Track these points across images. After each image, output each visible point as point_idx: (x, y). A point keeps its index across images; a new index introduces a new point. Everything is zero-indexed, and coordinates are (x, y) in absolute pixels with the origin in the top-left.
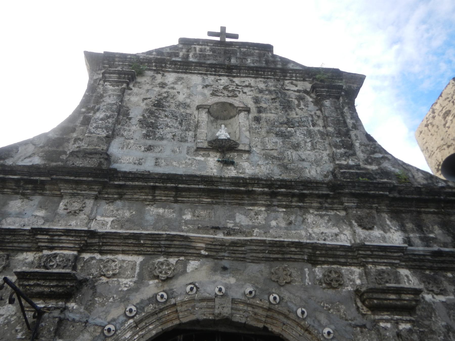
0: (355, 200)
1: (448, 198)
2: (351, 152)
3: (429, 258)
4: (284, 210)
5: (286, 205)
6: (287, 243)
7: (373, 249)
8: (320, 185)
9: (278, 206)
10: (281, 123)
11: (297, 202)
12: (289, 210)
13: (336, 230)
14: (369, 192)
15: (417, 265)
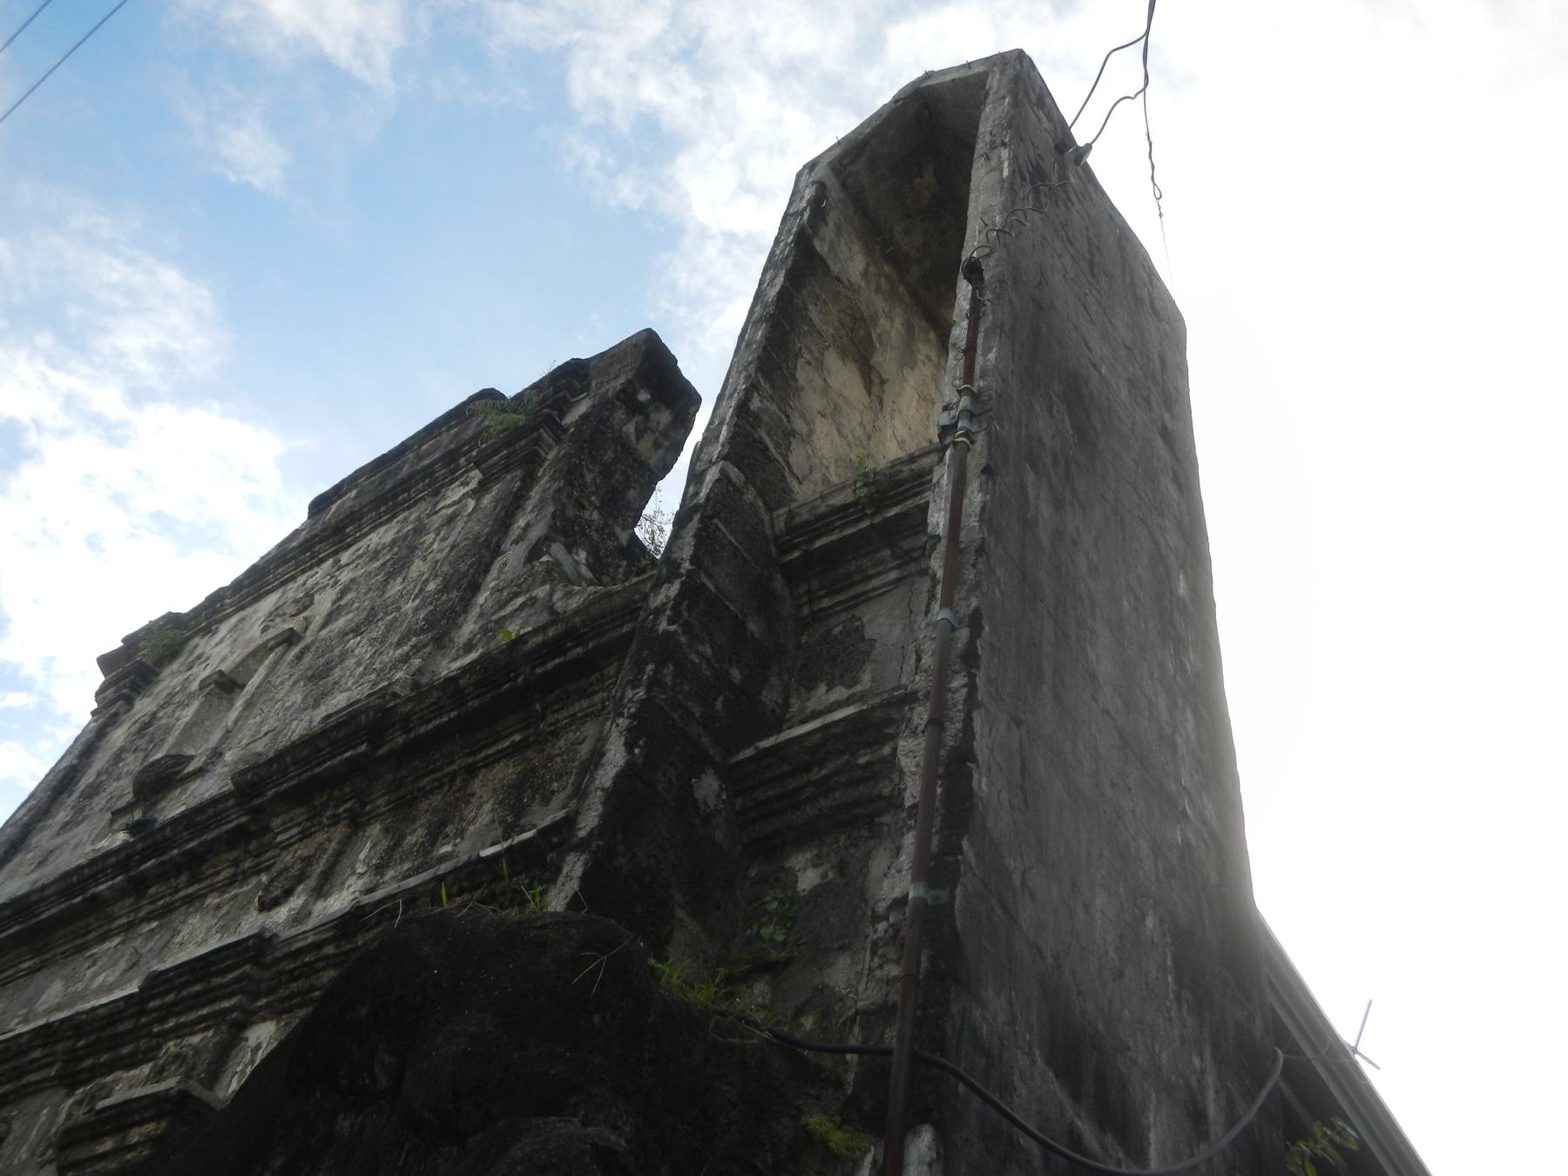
0: (300, 813)
1: (538, 671)
3: (330, 950)
6: (27, 1036)
7: (177, 982)
8: (221, 806)
11: (190, 883)
14: (316, 771)
15: (292, 996)
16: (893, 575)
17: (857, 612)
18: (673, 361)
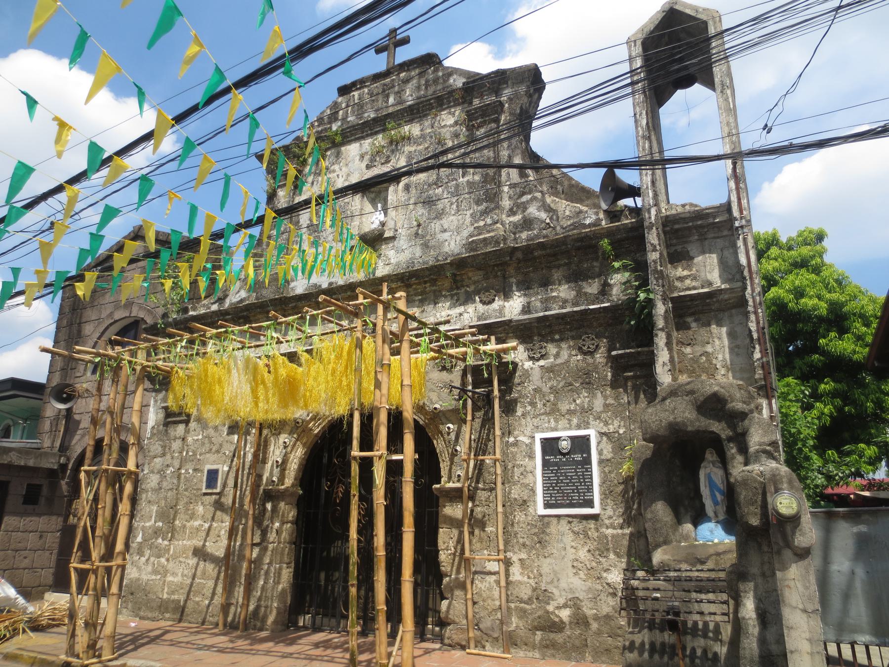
0: (481, 273)
2: (493, 206)
4: (420, 297)
5: (421, 292)
9: (416, 295)
10: (430, 185)
12: (424, 296)
13: (461, 309)
16: (696, 237)
17: (686, 245)
18: (540, 73)
